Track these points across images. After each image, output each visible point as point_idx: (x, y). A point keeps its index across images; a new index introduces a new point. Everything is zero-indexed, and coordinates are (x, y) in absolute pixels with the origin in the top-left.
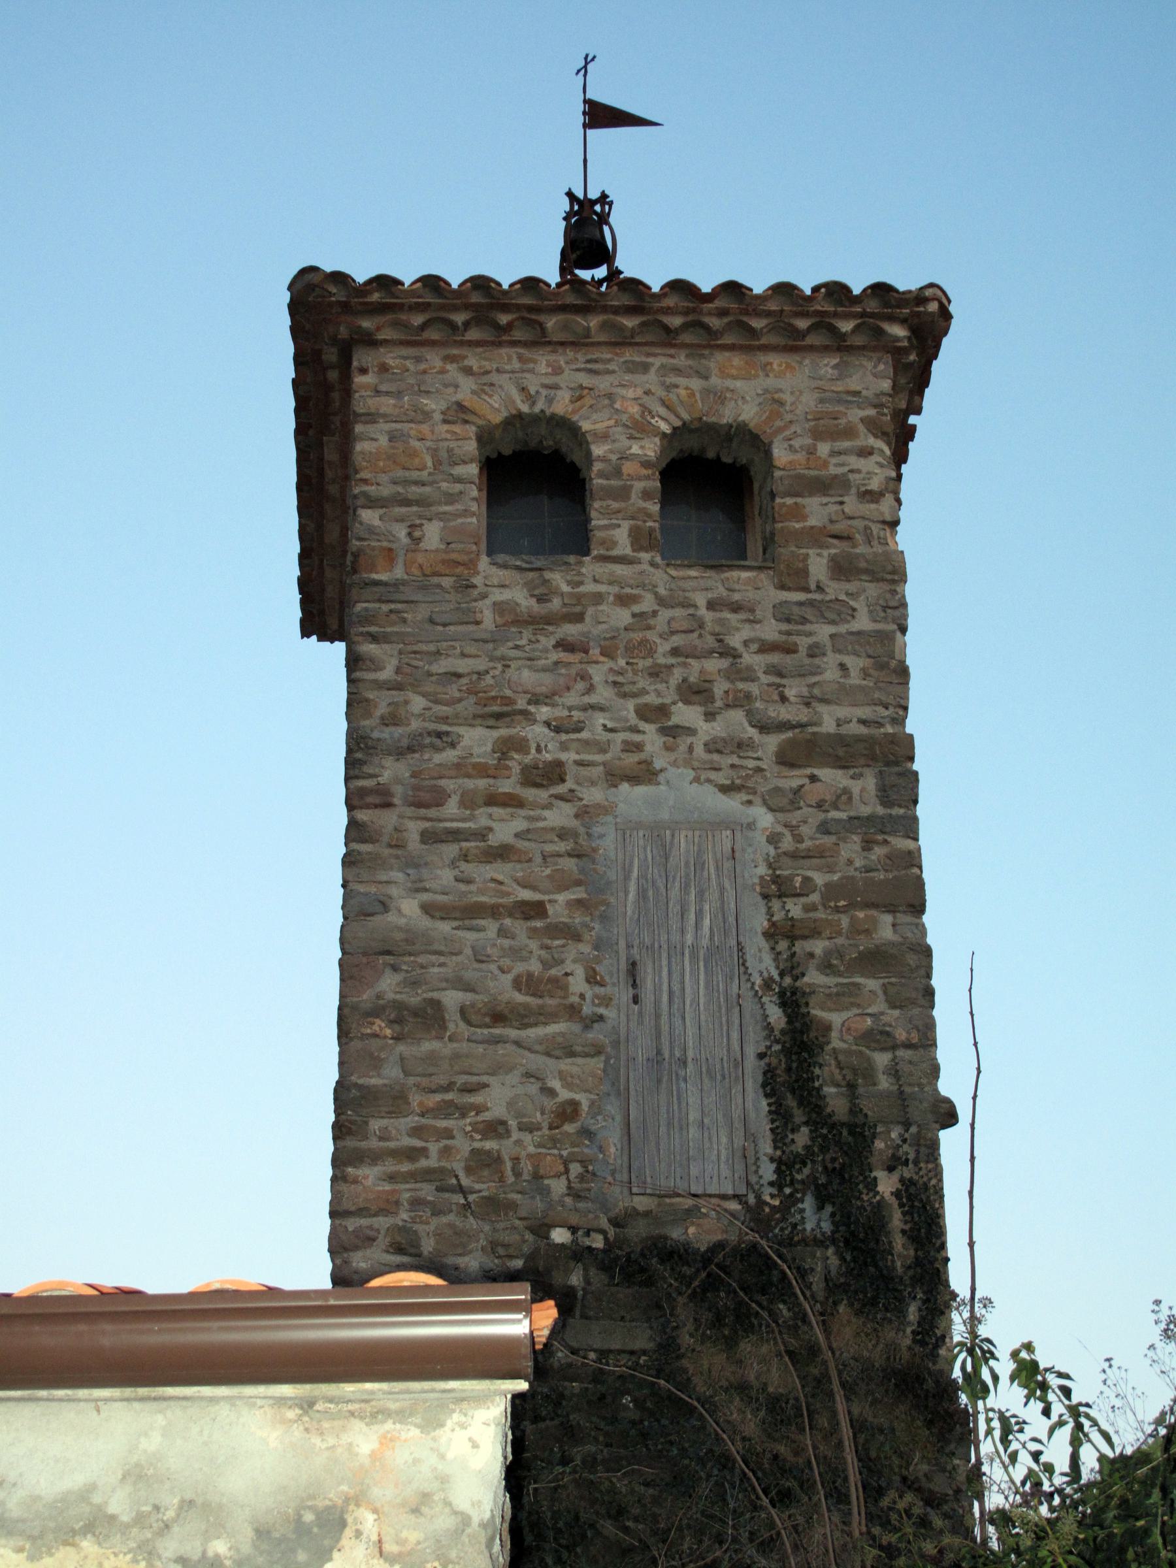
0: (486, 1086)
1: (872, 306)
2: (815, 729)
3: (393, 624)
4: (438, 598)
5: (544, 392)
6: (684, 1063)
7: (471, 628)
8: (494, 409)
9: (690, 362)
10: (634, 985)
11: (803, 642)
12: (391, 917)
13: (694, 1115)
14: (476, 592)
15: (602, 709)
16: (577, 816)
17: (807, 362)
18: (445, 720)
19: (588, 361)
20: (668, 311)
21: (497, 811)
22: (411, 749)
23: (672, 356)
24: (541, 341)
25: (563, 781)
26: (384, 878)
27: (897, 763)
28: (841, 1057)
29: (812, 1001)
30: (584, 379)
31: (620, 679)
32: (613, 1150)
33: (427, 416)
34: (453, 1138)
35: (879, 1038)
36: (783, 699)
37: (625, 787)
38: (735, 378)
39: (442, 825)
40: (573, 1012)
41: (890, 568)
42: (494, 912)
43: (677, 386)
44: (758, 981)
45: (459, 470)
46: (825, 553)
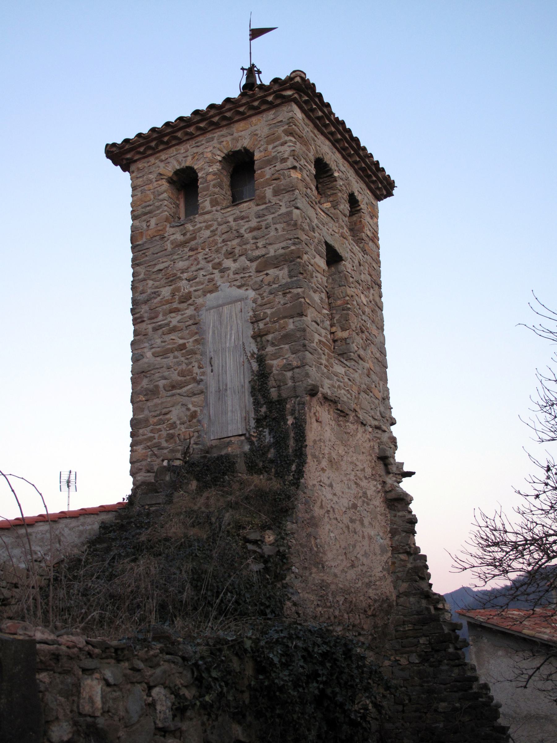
0: (170, 411)
1: (276, 87)
2: (268, 256)
3: (143, 258)
4: (155, 245)
5: (184, 159)
6: (226, 390)
7: (164, 252)
8: (169, 171)
9: (227, 131)
10: (212, 366)
11: (263, 224)
12: (145, 360)
13: (230, 408)
14: (166, 239)
15: (202, 269)
16: (195, 310)
17: (264, 116)
18: (157, 287)
19: (196, 143)
20: (213, 116)
21: (173, 315)
22: (148, 301)
23: (221, 131)
24: (180, 142)
25: (191, 298)
26: (142, 347)
27: (294, 261)
28: (275, 377)
29: (267, 358)
30: (195, 150)
31: (206, 257)
32: (206, 425)
33: (151, 181)
34: (161, 431)
35: (289, 367)
36: (257, 248)
37: (208, 295)
38: (242, 131)
39: (157, 324)
40: (194, 380)
41: (291, 186)
42: (172, 351)
43: (223, 142)
44: (249, 355)
45: (161, 197)
46: (271, 187)
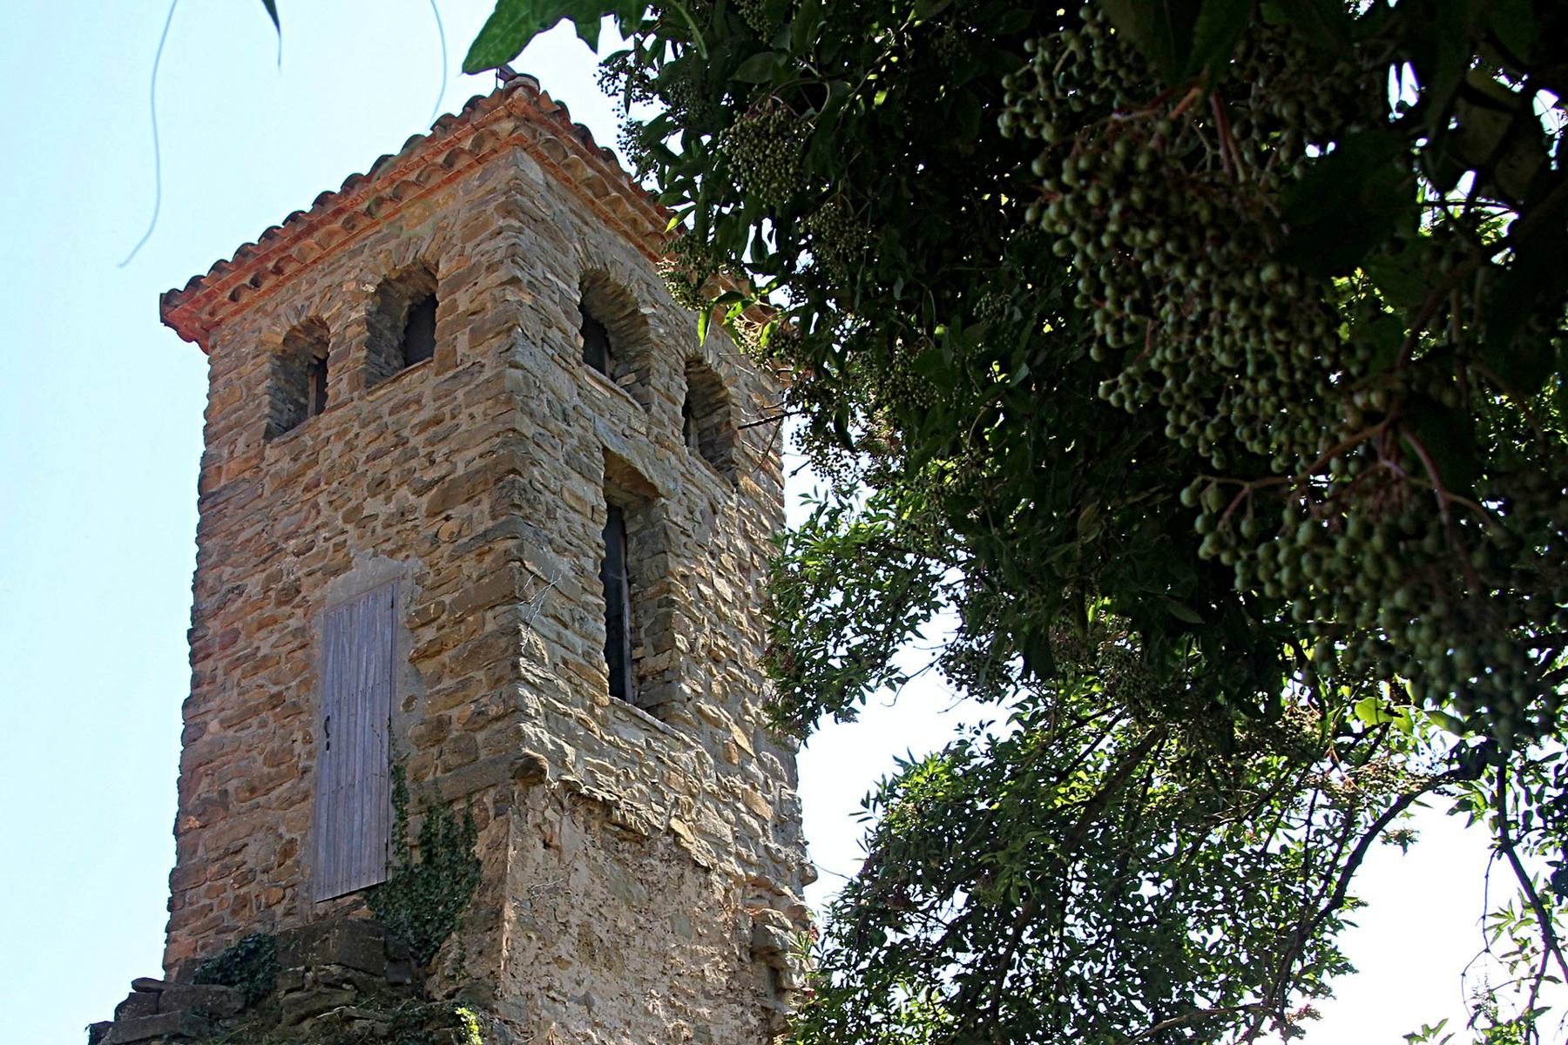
42: (255, 711)
